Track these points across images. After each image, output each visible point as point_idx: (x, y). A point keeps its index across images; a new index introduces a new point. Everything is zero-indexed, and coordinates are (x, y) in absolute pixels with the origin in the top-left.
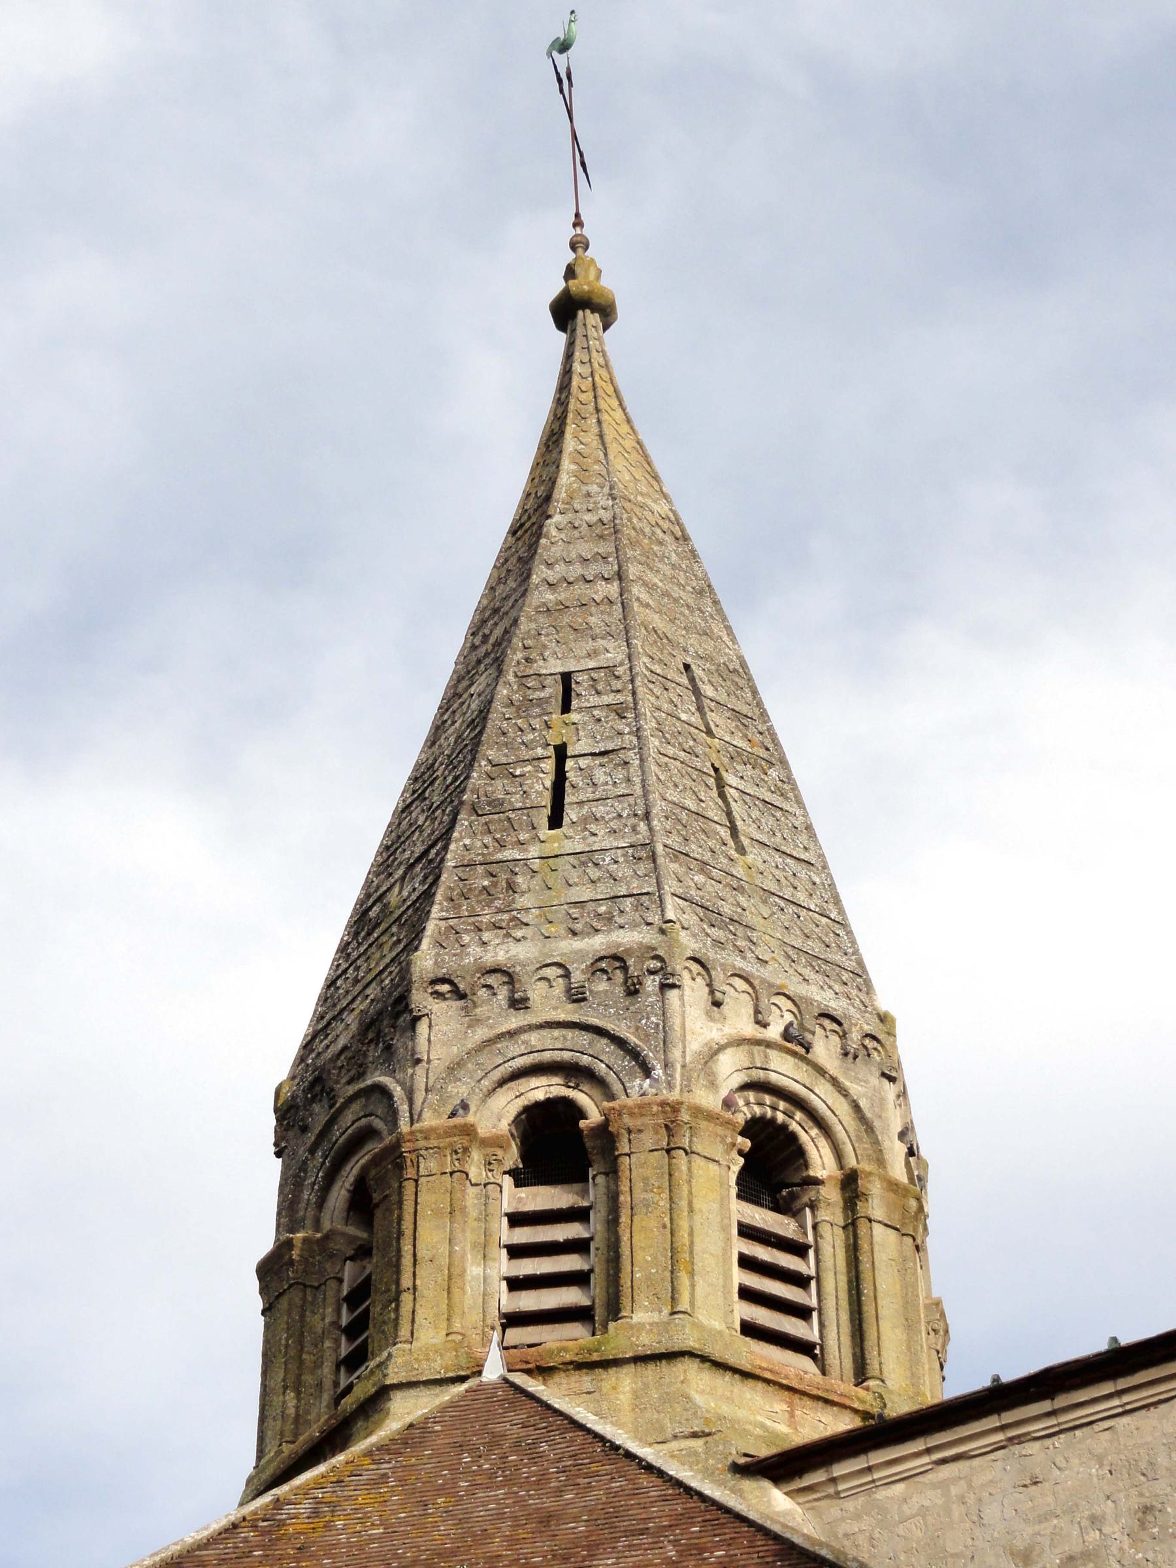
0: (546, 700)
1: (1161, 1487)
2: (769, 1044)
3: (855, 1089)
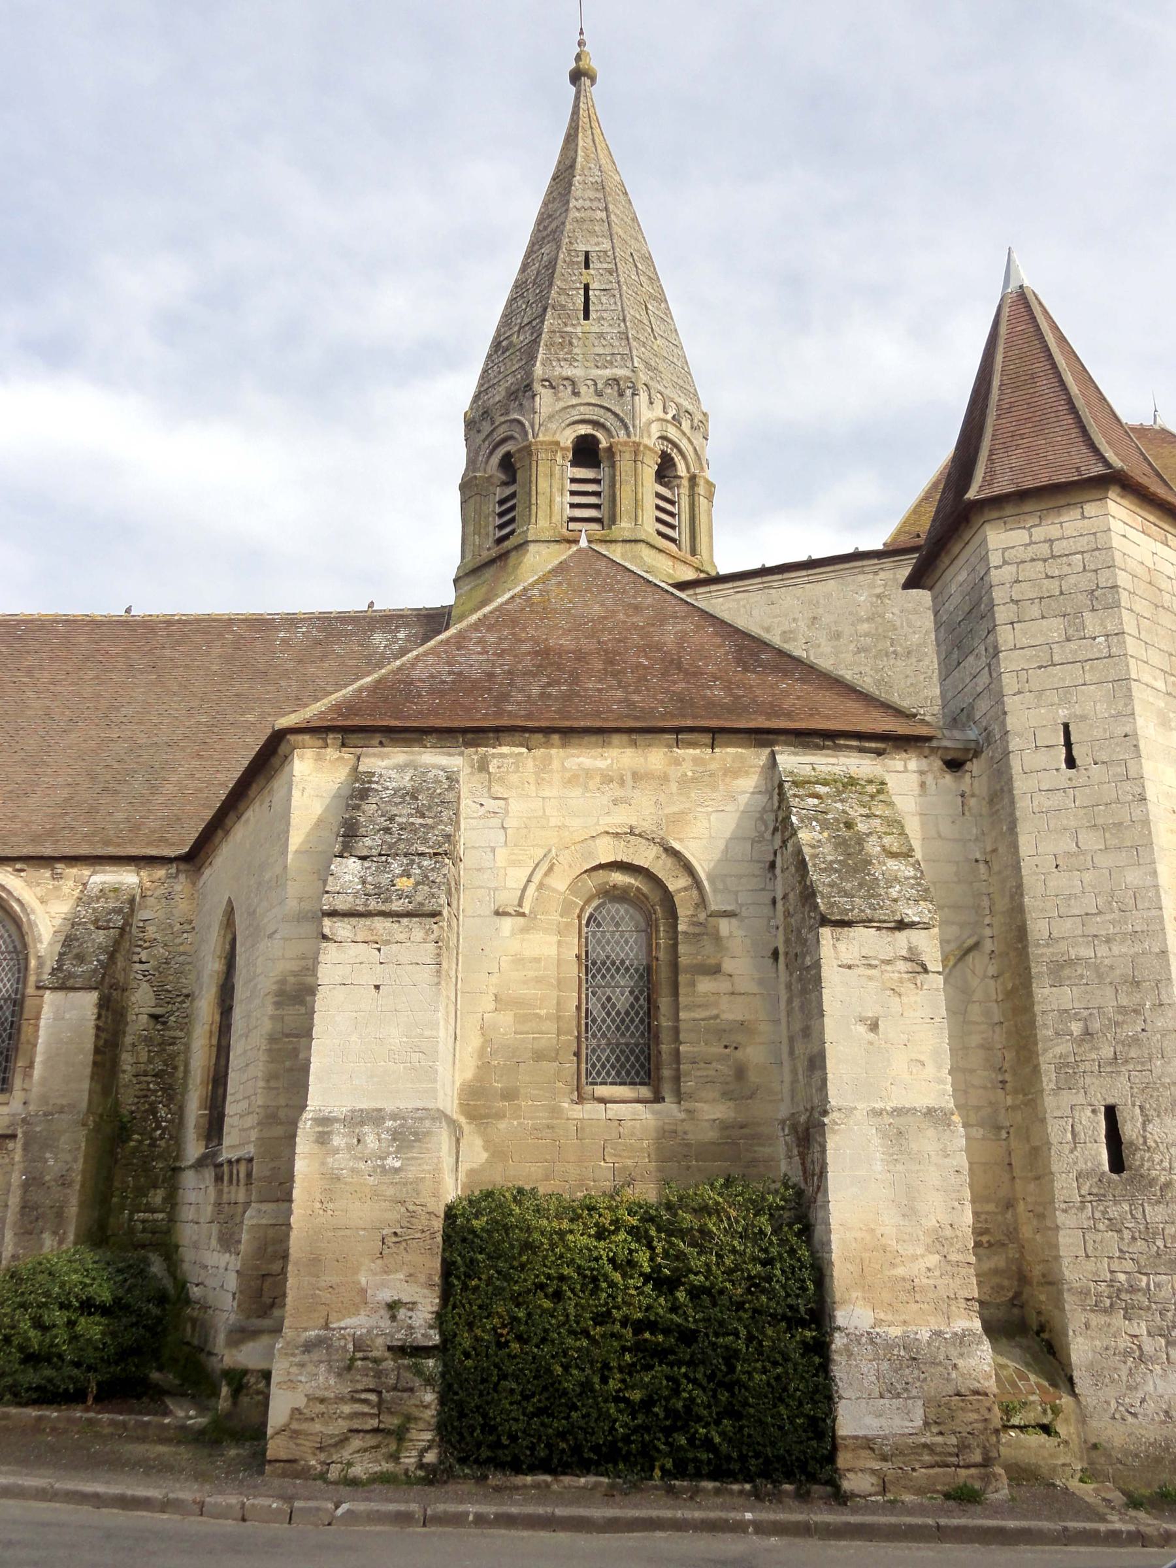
0: (578, 263)
1: (821, 611)
2: (667, 421)
3: (695, 442)
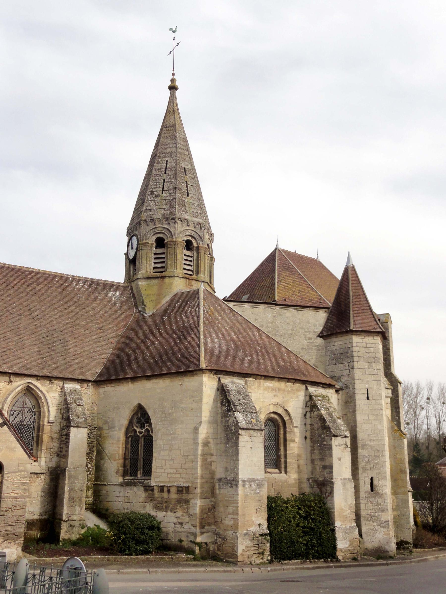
1: (258, 317)
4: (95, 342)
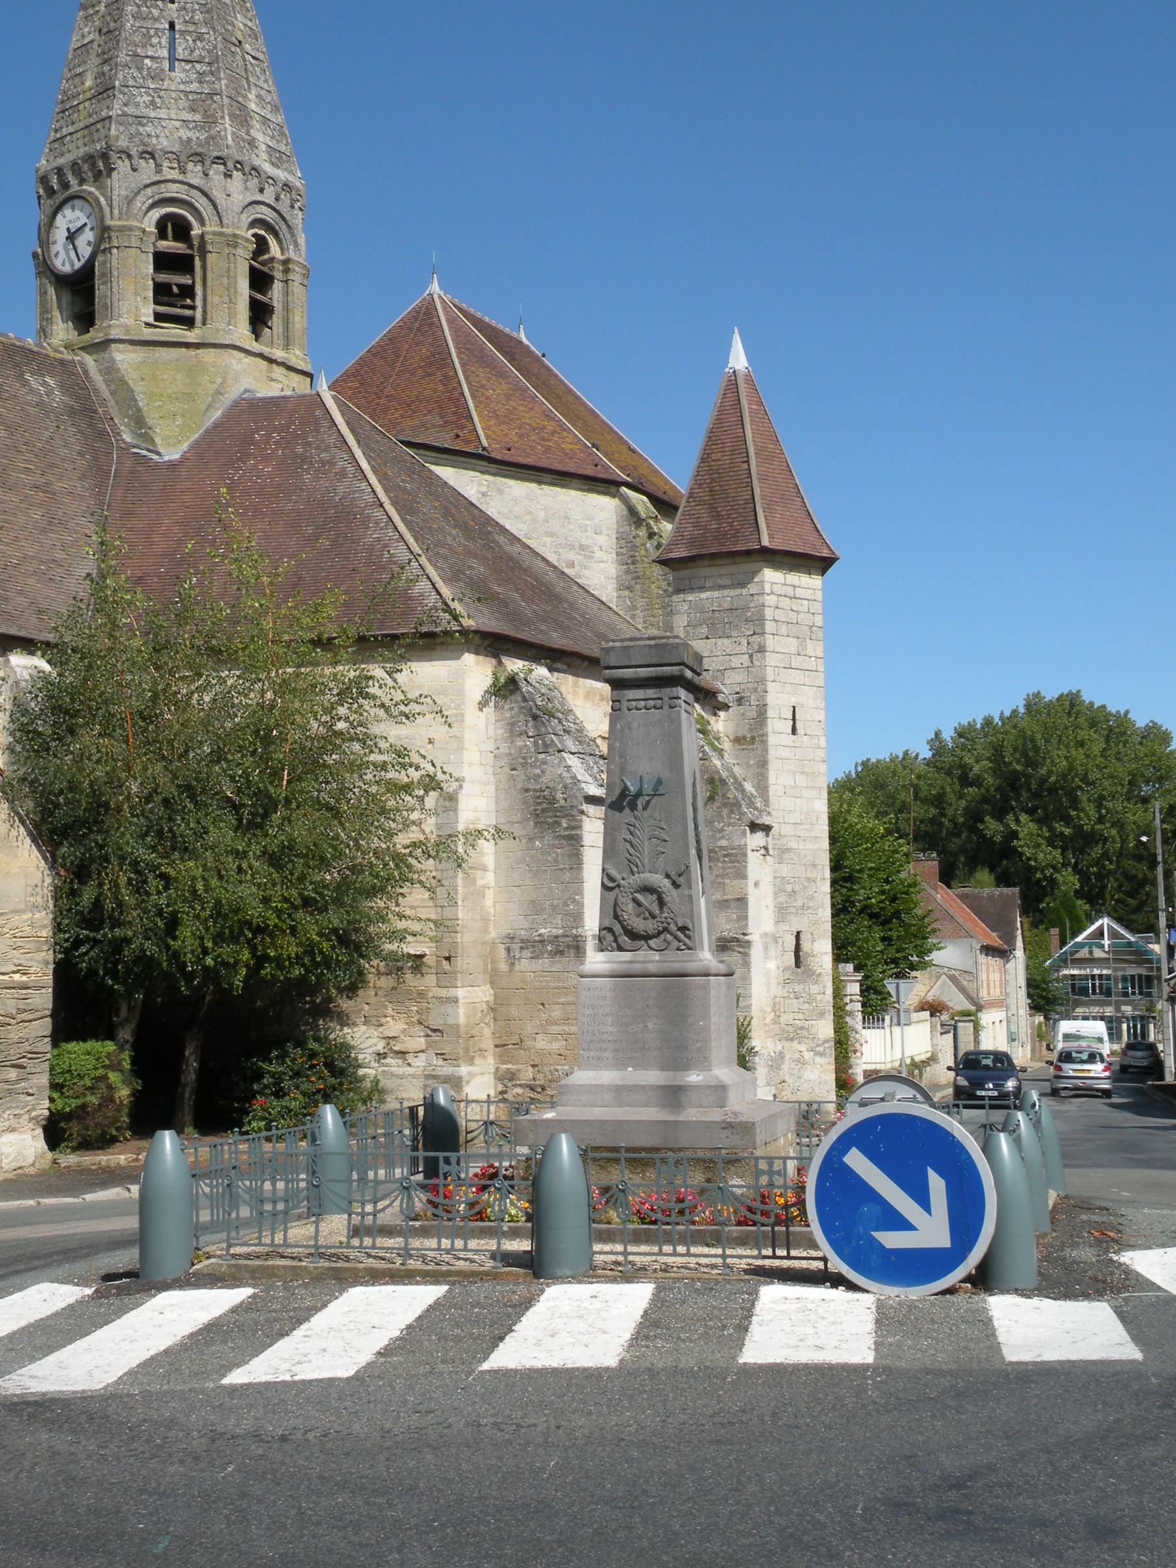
4: (44, 531)
